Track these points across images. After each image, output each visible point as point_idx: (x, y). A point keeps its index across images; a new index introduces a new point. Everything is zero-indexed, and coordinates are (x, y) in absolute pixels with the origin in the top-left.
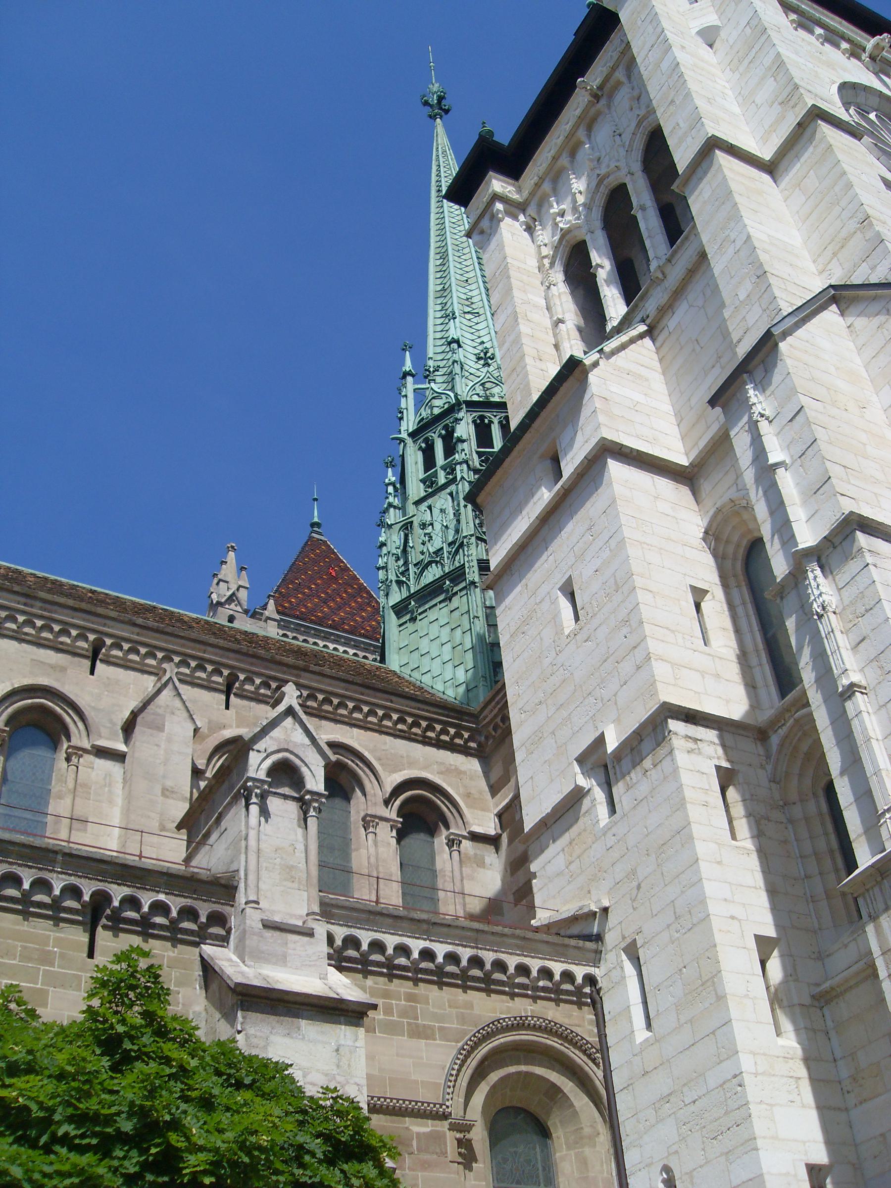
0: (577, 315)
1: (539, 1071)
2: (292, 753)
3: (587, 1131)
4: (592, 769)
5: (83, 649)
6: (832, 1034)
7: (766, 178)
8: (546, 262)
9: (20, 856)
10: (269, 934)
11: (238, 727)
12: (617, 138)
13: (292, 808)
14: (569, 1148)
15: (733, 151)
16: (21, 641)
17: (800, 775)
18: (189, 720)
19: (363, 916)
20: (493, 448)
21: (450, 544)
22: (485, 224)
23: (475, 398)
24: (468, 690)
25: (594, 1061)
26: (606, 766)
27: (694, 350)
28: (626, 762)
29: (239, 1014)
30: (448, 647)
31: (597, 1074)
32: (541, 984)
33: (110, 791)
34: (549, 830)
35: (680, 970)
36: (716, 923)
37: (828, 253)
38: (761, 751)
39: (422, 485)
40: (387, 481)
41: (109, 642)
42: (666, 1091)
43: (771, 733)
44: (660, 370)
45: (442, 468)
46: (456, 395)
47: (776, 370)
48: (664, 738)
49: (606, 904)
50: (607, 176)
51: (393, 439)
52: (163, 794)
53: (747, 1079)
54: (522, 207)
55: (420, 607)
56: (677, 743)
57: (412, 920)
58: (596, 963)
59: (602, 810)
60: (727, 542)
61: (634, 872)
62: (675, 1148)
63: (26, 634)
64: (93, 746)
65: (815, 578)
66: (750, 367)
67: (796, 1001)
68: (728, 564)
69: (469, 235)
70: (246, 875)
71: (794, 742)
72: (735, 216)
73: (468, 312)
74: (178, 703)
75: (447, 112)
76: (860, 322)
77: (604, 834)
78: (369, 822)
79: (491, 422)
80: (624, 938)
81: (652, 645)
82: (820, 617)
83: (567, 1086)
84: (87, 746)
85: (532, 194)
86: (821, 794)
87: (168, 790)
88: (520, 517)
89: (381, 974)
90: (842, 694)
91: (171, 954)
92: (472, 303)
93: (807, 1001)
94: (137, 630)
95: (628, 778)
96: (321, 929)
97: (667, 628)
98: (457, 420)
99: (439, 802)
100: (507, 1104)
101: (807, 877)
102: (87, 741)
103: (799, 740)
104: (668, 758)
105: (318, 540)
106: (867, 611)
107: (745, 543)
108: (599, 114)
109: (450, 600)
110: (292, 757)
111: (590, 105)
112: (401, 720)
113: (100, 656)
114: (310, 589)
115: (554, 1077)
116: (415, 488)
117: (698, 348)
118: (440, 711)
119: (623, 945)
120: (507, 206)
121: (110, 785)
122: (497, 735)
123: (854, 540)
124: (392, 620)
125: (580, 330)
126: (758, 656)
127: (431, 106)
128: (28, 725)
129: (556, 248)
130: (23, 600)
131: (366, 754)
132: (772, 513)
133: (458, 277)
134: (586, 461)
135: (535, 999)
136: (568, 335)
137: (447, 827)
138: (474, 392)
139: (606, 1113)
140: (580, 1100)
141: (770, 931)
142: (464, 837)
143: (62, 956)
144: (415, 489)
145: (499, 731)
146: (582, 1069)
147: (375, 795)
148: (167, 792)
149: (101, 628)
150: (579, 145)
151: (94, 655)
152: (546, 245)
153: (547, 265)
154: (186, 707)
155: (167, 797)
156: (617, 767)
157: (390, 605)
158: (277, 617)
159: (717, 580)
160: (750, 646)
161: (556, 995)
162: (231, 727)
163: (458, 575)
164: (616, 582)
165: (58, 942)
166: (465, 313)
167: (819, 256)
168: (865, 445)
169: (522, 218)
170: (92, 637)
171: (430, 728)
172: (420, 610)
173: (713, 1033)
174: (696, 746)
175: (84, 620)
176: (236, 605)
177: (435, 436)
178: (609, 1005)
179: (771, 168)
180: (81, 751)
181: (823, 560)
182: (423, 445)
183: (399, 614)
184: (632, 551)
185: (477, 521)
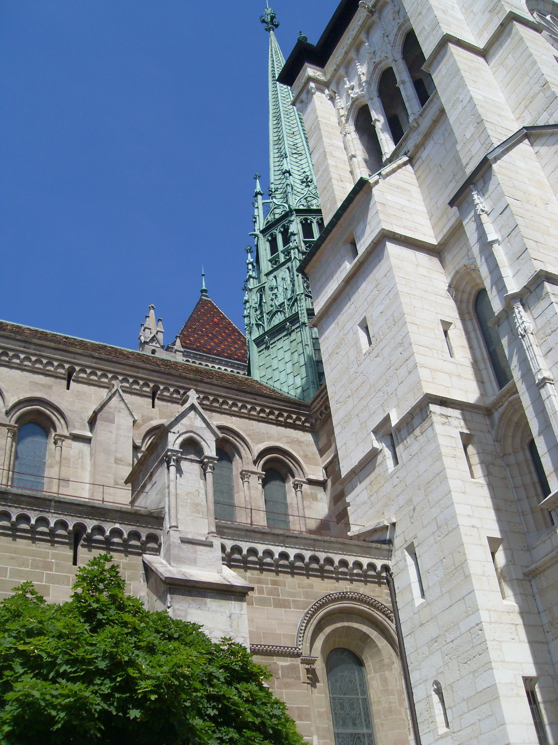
0: (364, 152)
1: (355, 625)
2: (195, 433)
3: (386, 661)
4: (382, 437)
5: (61, 373)
6: (537, 597)
7: (481, 60)
8: (343, 119)
9: (29, 504)
10: (184, 546)
11: (160, 419)
12: (386, 38)
13: (196, 467)
14: (376, 672)
16: (23, 370)
17: (513, 437)
18: (130, 416)
19: (243, 533)
20: (314, 238)
21: (289, 300)
22: (304, 96)
23: (301, 207)
24: (303, 391)
25: (389, 618)
26: (391, 435)
27: (438, 171)
28: (404, 432)
29: (169, 596)
30: (290, 364)
32: (355, 571)
33: (82, 462)
34: (357, 476)
35: (442, 560)
36: (463, 530)
37: (522, 106)
38: (488, 421)
39: (270, 263)
40: (248, 261)
41: (77, 368)
42: (434, 636)
43: (494, 410)
44: (417, 185)
45: (282, 252)
46: (289, 206)
47: (491, 182)
48: (427, 416)
49: (394, 520)
50: (380, 62)
51: (251, 235)
52: (116, 462)
53: (485, 626)
54: (327, 85)
55: (271, 340)
56: (435, 419)
57: (274, 534)
58: (389, 557)
59: (390, 462)
60: (463, 292)
61: (411, 500)
62: (441, 670)
63: (26, 366)
64: (71, 434)
65: (519, 312)
66: (474, 181)
67: (514, 577)
68: (464, 306)
69: (293, 104)
70: (169, 510)
71: (509, 416)
72: (462, 85)
73: (295, 153)
74: (122, 405)
75: (277, 26)
76: (543, 150)
77: (392, 477)
78: (244, 475)
79: (312, 222)
80: (406, 541)
81: (418, 358)
82: (523, 336)
83: (373, 634)
84: (67, 434)
85: (333, 76)
86: (526, 447)
87: (118, 459)
88: (332, 281)
89: (255, 569)
90: (538, 385)
91: (124, 561)
92: (297, 147)
93: (521, 576)
94: (95, 360)
95: (405, 442)
96: (217, 542)
97: (427, 347)
98: (291, 222)
99: (287, 461)
100: (336, 647)
101: (519, 500)
102: (67, 431)
103: (512, 414)
104: (430, 429)
105: (206, 300)
106: (552, 332)
107: (474, 292)
108: (374, 23)
109: (290, 335)
110: (195, 436)
112: (262, 411)
113: (73, 378)
114: (202, 331)
115: (365, 629)
116: (265, 265)
117: (441, 170)
118: (286, 404)
119: (405, 546)
120: (318, 85)
121: (82, 457)
122: (322, 418)
123: (543, 288)
124: (254, 349)
125: (366, 161)
126: (485, 363)
127: (267, 23)
128: (30, 422)
129: (349, 110)
130: (23, 344)
131: (241, 433)
132: (491, 273)
133: (288, 131)
134: (373, 244)
135: (352, 581)
136: (359, 165)
137: (293, 476)
138: (300, 204)
139: (398, 650)
140: (382, 643)
141: (497, 534)
142: (304, 482)
143: (57, 564)
144: (266, 266)
145: (324, 416)
146: (382, 623)
147: (247, 458)
148: (118, 461)
149: (72, 360)
150: (361, 43)
151: (69, 377)
152: (342, 108)
153: (344, 121)
154: (128, 408)
155: (118, 464)
156: (398, 435)
157: (253, 339)
158: (182, 350)
159: (457, 316)
160: (479, 357)
161: (365, 578)
162: (156, 419)
163: (294, 319)
164: (394, 319)
165: (55, 556)
166: (293, 154)
167: (516, 108)
168: (548, 227)
169: (327, 92)
170: (67, 366)
171: (280, 415)
172: (271, 342)
173: (463, 598)
174: (447, 421)
175: (61, 355)
176: (156, 343)
177: (277, 232)
178: (398, 584)
179: (484, 53)
180: (63, 437)
181: (524, 300)
182: (270, 238)
183: (258, 345)
184: (403, 299)
185: (305, 285)
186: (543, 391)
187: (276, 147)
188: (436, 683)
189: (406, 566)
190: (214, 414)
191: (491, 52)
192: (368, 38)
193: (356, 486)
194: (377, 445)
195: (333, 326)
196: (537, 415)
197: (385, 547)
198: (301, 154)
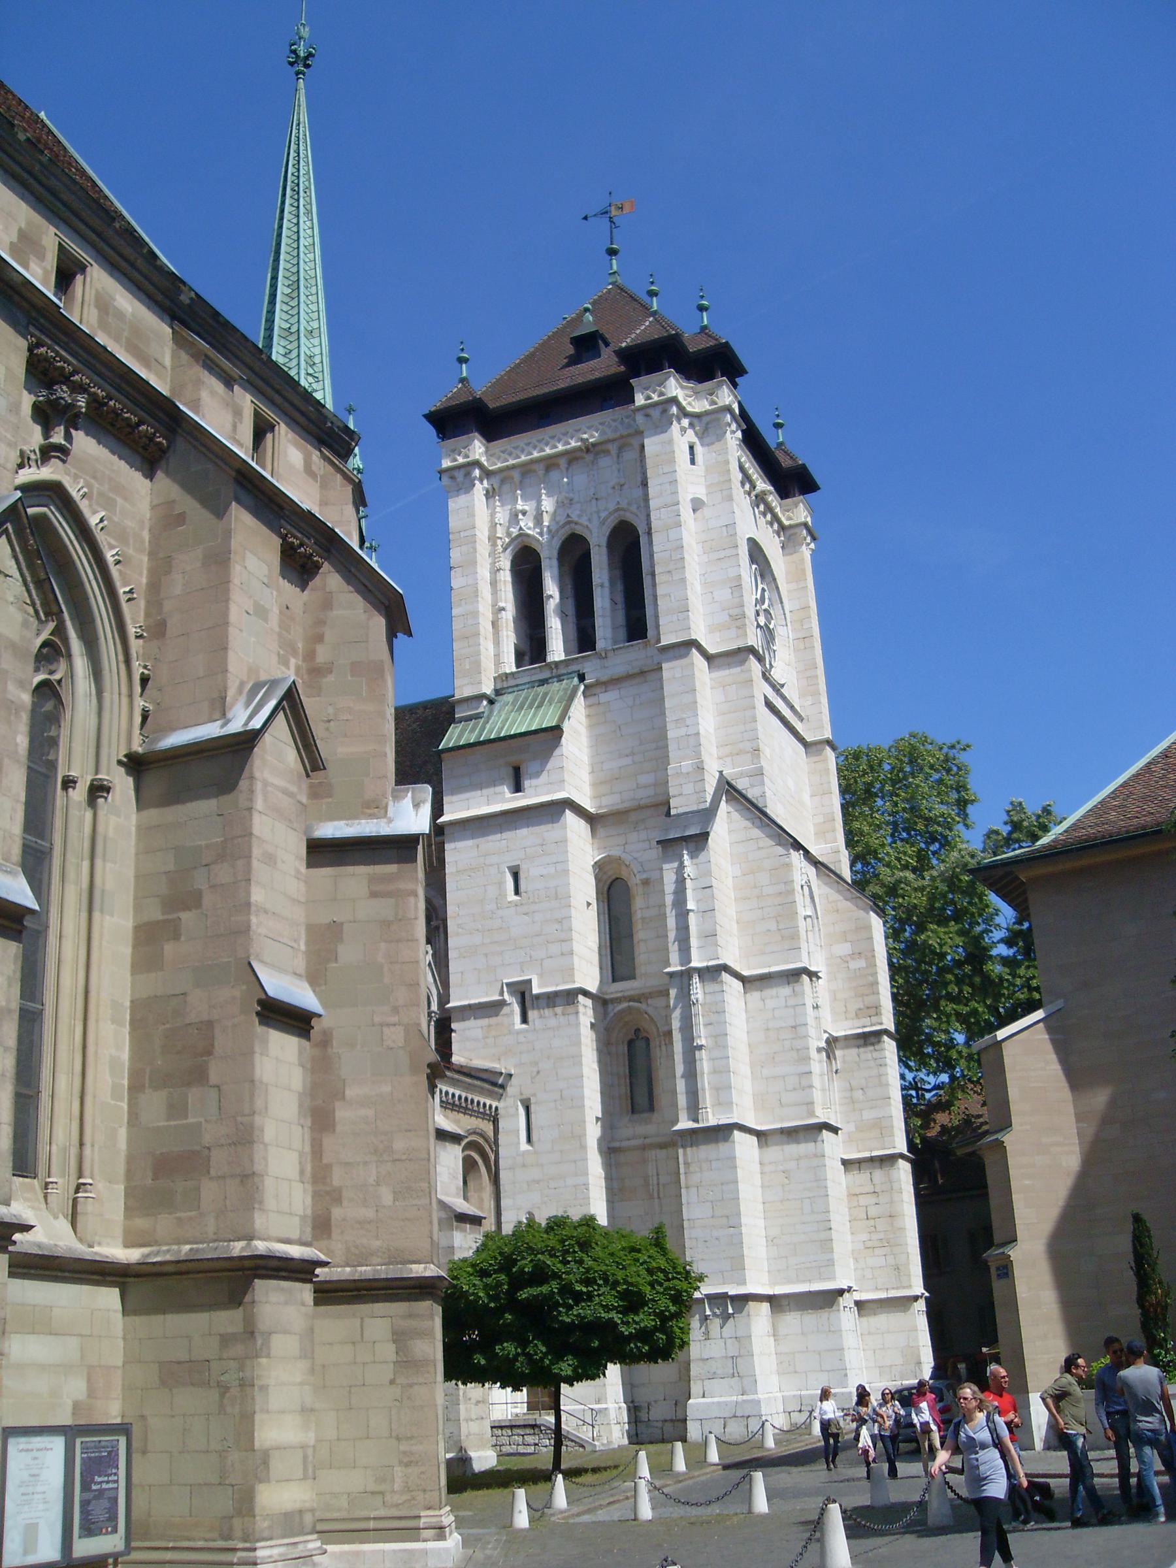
26: (523, 995)
28: (543, 1002)
31: (492, 1157)
44: (585, 724)
59: (517, 1018)
60: (605, 873)
61: (536, 1063)
73: (311, 375)
80: (521, 1094)
85: (501, 470)
86: (626, 1043)
88: (479, 792)
107: (614, 877)
108: (582, 458)
111: (578, 449)
127: (297, 56)
129: (513, 540)
135: (477, 1117)
139: (493, 1177)
141: (600, 1116)
153: (500, 549)
160: (603, 944)
166: (308, 374)
169: (485, 482)
178: (502, 1124)
179: (709, 658)
186: (697, 1052)
187: (283, 343)
188: (529, 1213)
189: (518, 1114)
191: (717, 661)
192: (567, 469)
193: (469, 1019)
194: (506, 996)
195: (470, 843)
196: (684, 1062)
197: (501, 1091)
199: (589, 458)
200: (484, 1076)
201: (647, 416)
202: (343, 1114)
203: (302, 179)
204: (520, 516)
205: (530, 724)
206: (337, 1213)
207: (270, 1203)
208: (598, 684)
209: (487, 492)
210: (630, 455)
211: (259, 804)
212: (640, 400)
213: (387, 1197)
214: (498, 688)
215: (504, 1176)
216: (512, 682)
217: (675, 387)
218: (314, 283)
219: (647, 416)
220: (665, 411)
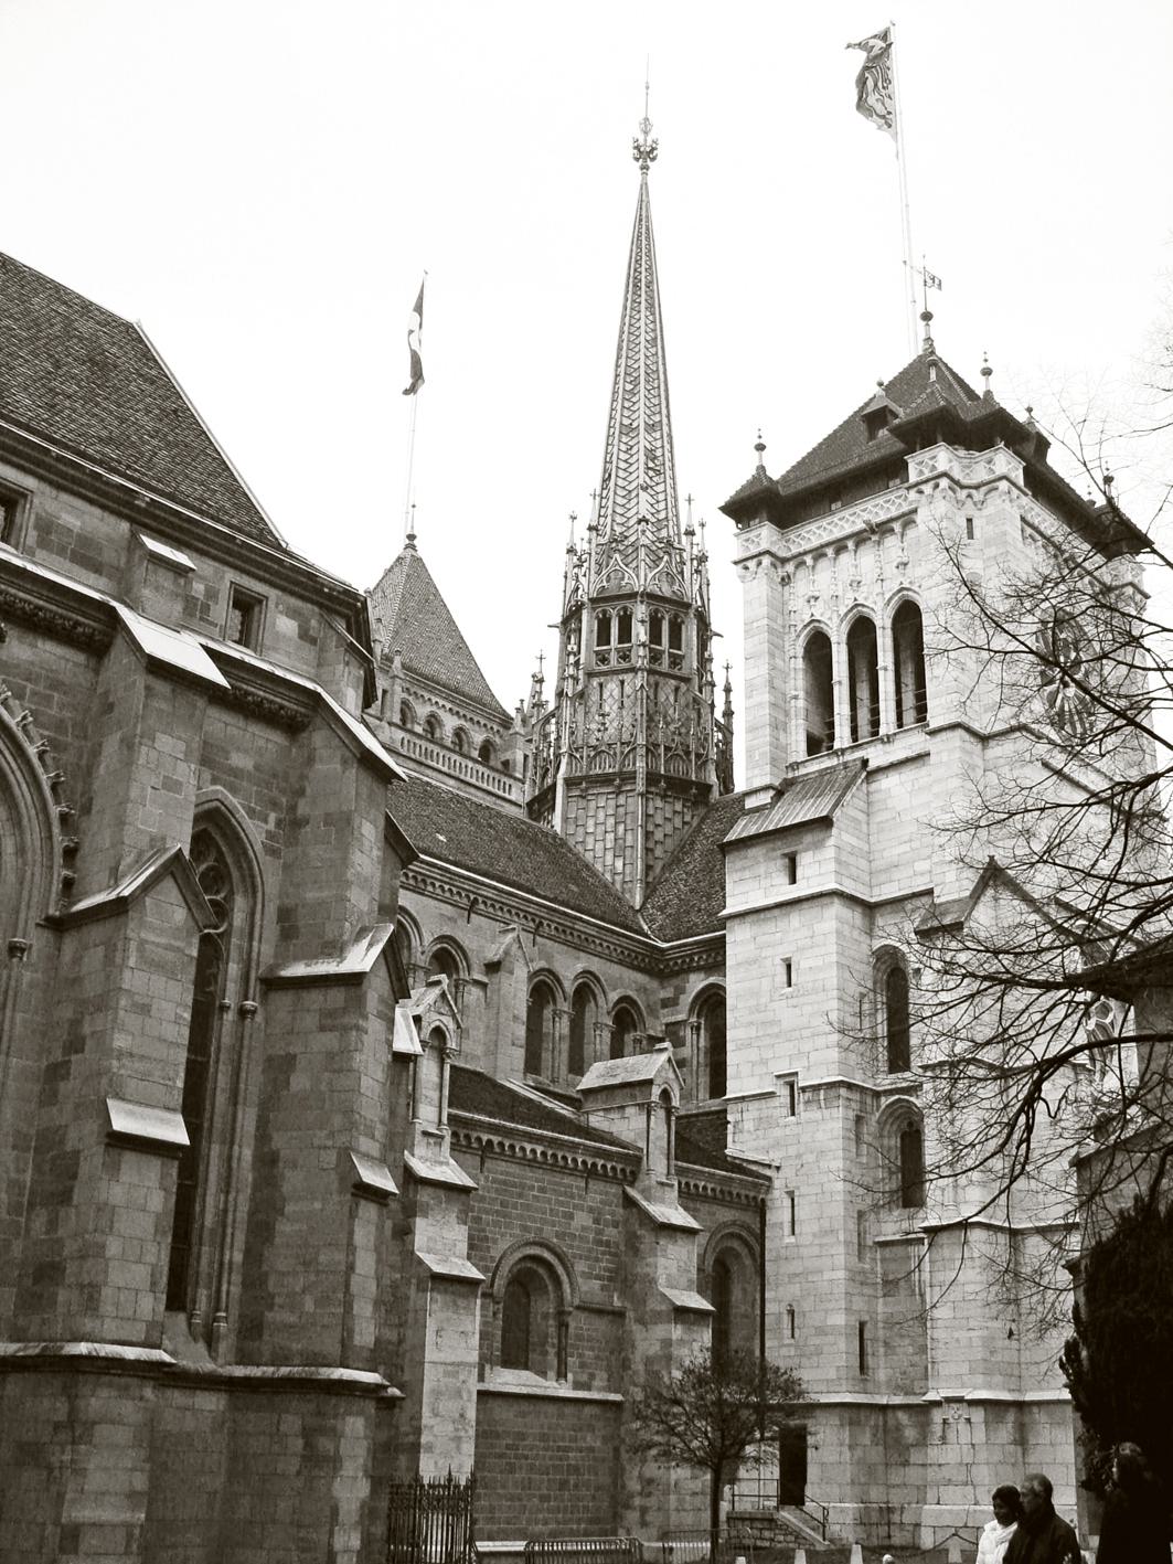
7: (980, 746)
15: (968, 730)
20: (660, 644)
22: (752, 564)
26: (792, 1086)
31: (757, 1248)
41: (480, 899)
50: (863, 606)
74: (520, 953)
75: (653, 159)
79: (663, 617)
85: (794, 557)
109: (617, 795)
111: (865, 530)
129: (806, 626)
131: (602, 979)
140: (748, 1262)
148: (516, 1018)
163: (632, 777)
170: (472, 897)
187: (624, 439)
190: (582, 954)
191: (992, 743)
198: (658, 473)
199: (875, 538)
200: (754, 1168)
201: (921, 492)
202: (284, 1228)
203: (644, 274)
204: (812, 602)
205: (805, 814)
206: (269, 1315)
207: (107, 1308)
208: (880, 770)
209: (783, 579)
210: (911, 533)
211: (132, 962)
212: (913, 477)
213: (309, 1305)
214: (790, 775)
215: (769, 1267)
216: (802, 771)
217: (942, 457)
218: (655, 376)
219: (921, 492)
220: (937, 486)
